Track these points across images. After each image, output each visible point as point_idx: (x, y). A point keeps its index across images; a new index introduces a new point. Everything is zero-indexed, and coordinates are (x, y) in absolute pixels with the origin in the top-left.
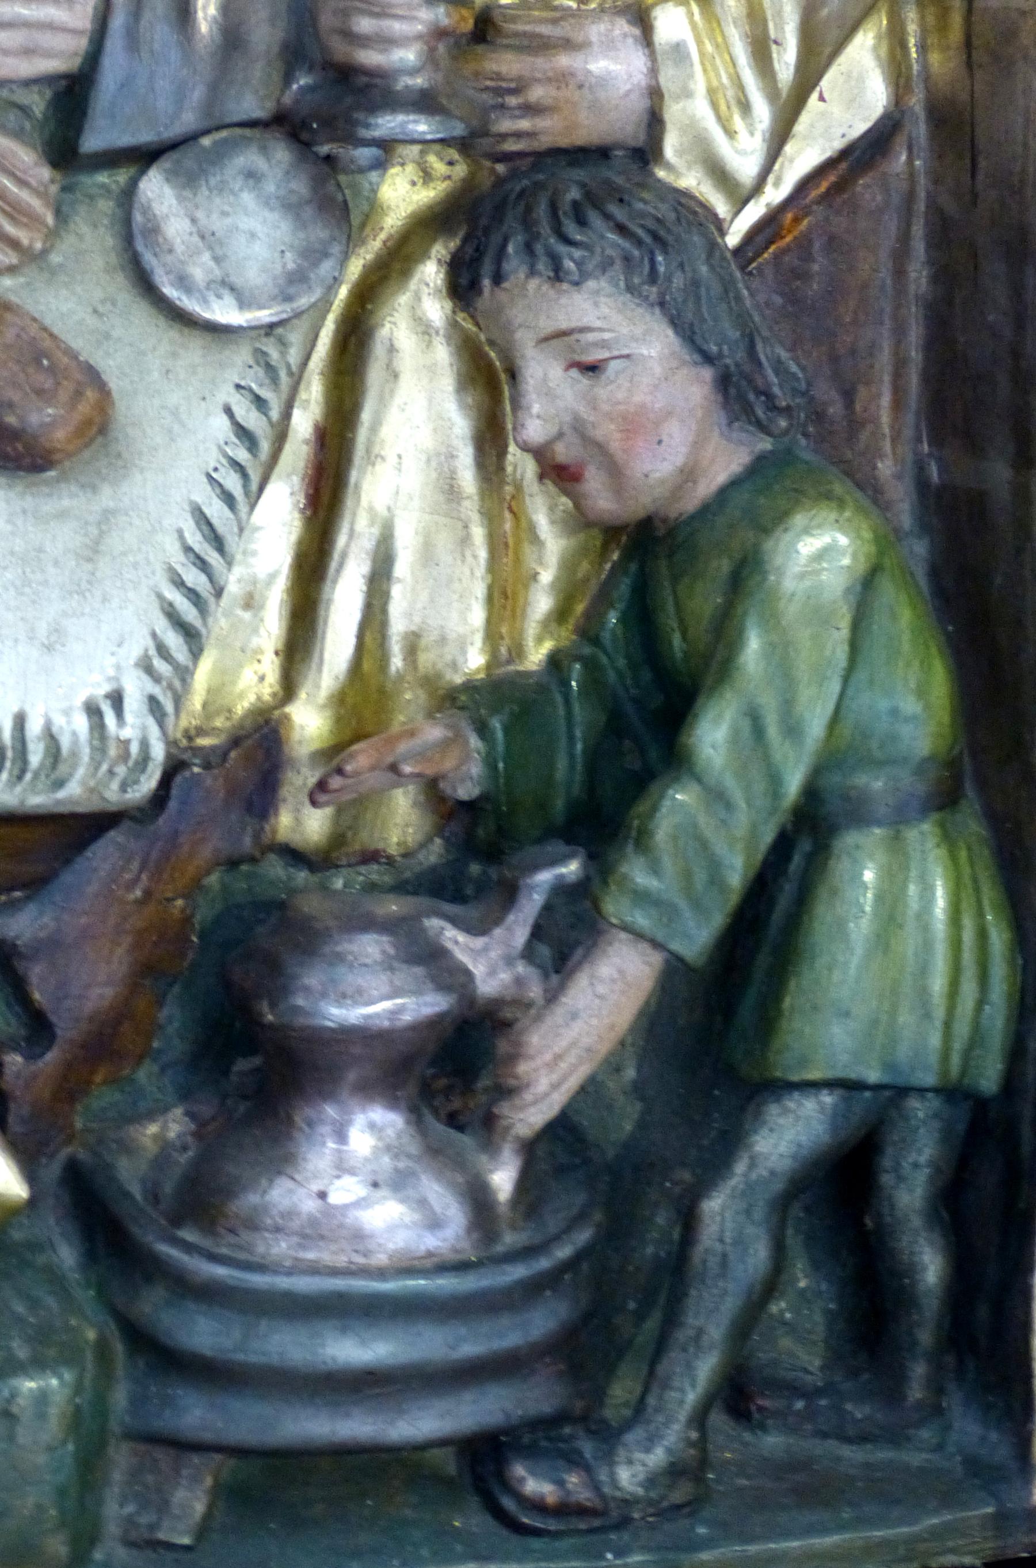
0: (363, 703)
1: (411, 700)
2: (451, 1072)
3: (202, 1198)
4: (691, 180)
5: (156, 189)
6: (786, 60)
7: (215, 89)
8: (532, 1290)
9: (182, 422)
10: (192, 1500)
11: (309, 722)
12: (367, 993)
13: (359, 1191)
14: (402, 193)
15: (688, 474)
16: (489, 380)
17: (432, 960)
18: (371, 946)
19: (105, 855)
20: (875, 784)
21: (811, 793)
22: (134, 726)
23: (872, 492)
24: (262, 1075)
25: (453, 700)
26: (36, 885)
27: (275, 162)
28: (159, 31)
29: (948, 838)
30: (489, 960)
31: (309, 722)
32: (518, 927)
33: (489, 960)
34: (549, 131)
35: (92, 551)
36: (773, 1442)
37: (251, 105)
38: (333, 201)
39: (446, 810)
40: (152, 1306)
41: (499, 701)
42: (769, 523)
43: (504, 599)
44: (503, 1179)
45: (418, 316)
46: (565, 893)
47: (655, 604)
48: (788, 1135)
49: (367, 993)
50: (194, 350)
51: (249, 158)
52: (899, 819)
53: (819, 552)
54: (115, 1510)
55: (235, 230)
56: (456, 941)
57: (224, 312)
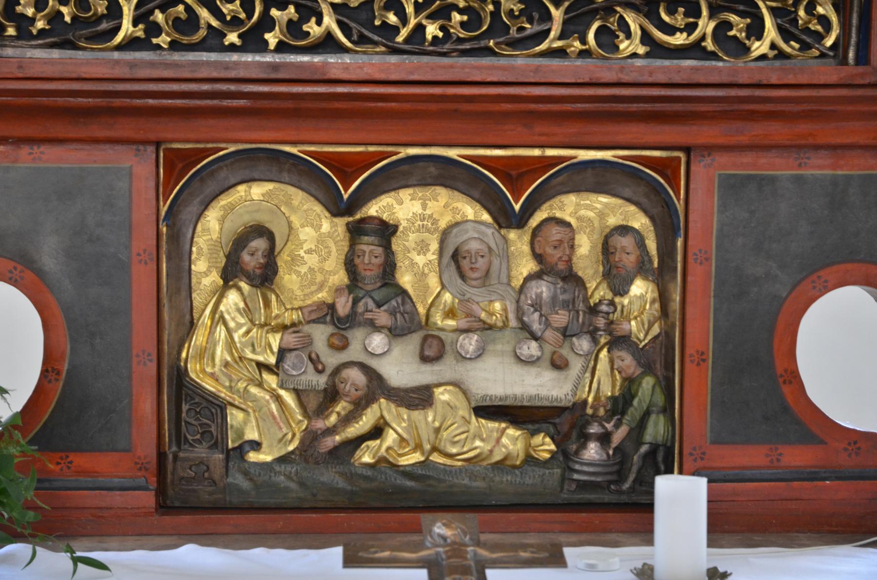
0: (597, 398)
1: (603, 399)
2: (604, 439)
3: (577, 453)
4: (635, 340)
5: (574, 339)
6: (646, 326)
7: (581, 329)
8: (615, 464)
9: (576, 365)
10: (574, 486)
11: (590, 400)
12: (594, 429)
13: (592, 451)
14: (603, 341)
15: (634, 373)
16: (612, 362)
17: (603, 427)
18: (596, 424)
19: (567, 416)
20: (654, 409)
21: (648, 408)
22: (570, 397)
23: (655, 375)
24: (584, 438)
25: (609, 398)
26: (559, 416)
27: (588, 337)
28: (575, 322)
29: (664, 417)
30: (609, 426)
31: (590, 400)
32: (612, 423)
33: (609, 426)
34: (619, 334)
35: (566, 378)
36: (644, 488)
37: (585, 330)
38: (595, 341)
39: (606, 411)
40: (571, 464)
41: (613, 399)
42: (642, 378)
43: (613, 386)
44: (611, 452)
45: (604, 353)
46: (618, 419)
47: (630, 386)
48: (644, 449)
49: (594, 429)
50: (578, 357)
51: (585, 336)
52: (658, 413)
53: (648, 382)
54: (566, 487)
55: (584, 344)
56: (607, 425)
57: (581, 353)
